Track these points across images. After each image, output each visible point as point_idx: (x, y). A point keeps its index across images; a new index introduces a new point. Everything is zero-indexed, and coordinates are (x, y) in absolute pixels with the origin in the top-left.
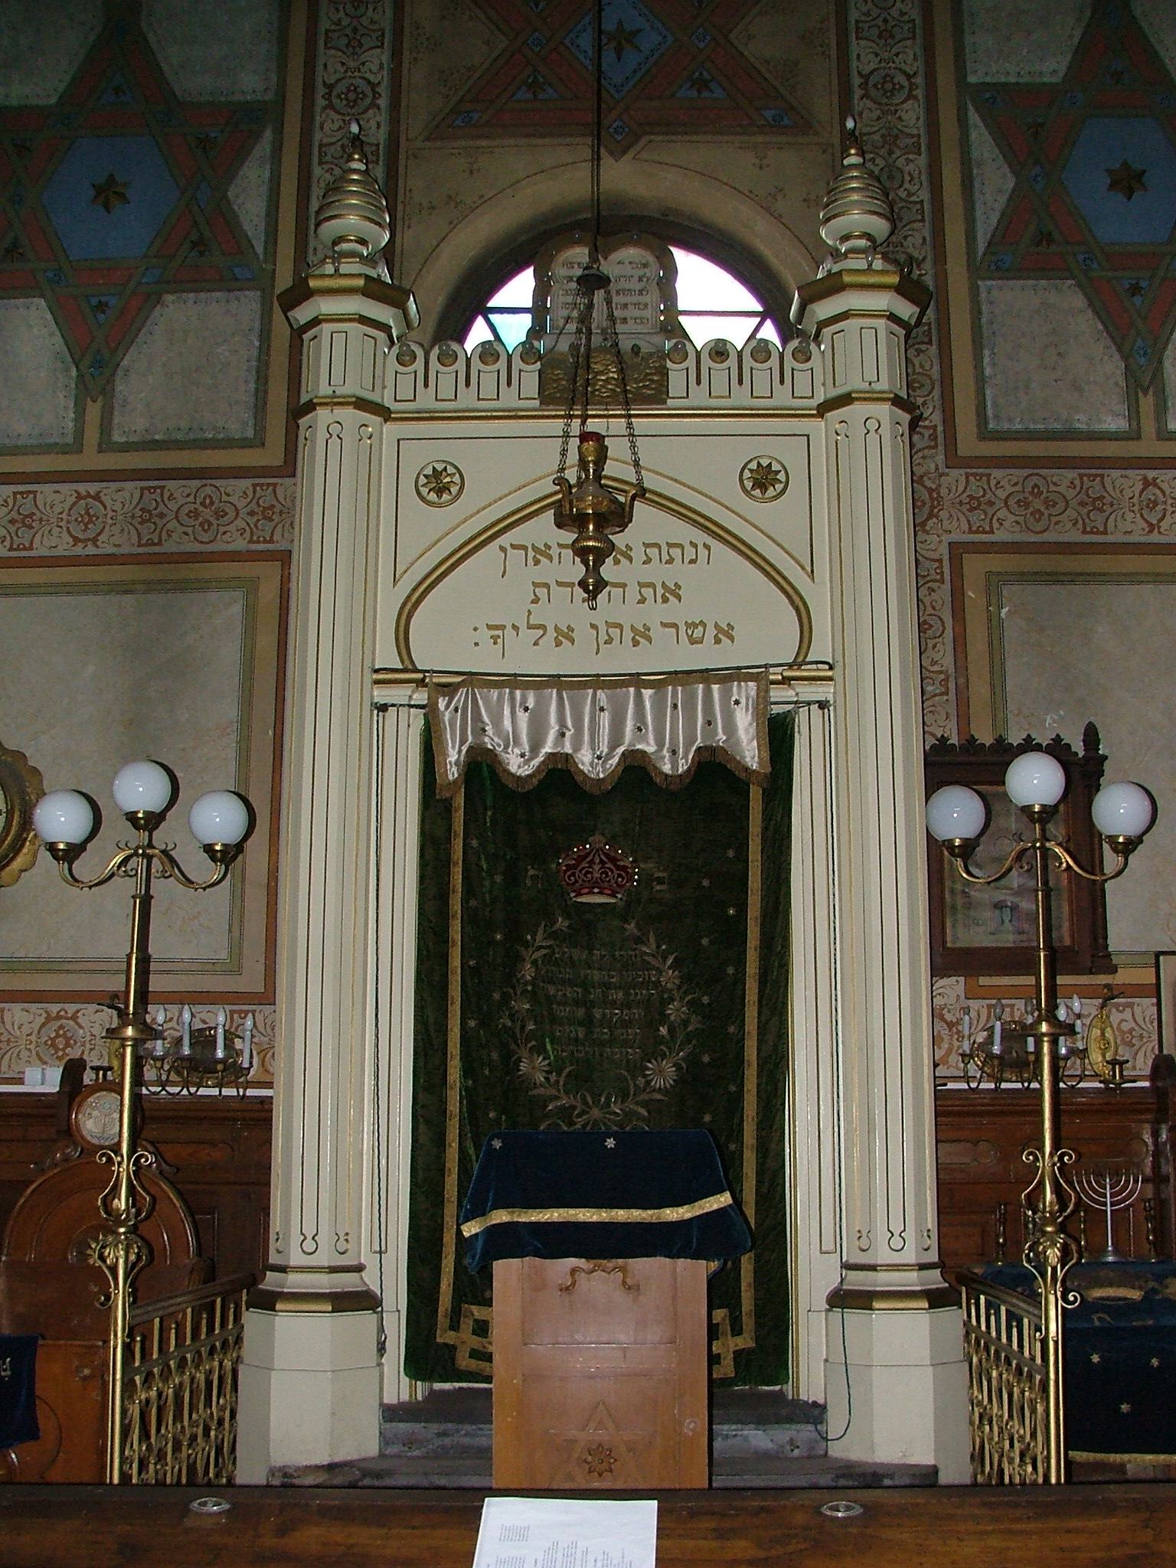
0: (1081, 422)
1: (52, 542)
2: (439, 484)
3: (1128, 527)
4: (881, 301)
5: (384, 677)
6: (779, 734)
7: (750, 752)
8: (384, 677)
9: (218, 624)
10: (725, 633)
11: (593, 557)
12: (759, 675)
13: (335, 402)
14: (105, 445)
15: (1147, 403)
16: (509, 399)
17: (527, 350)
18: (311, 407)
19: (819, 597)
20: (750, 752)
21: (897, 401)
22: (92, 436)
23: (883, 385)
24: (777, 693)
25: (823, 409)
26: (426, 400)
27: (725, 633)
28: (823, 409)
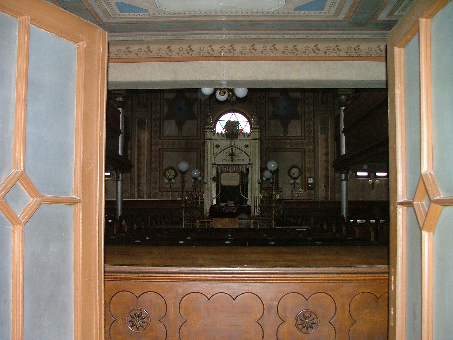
0: (279, 135)
1: (176, 146)
2: (218, 146)
3: (283, 146)
4: (257, 130)
5: (213, 164)
6: (247, 170)
7: (245, 171)
8: (214, 164)
9: (193, 155)
10: (243, 160)
11: (232, 158)
12: (246, 165)
13: (208, 139)
14: (182, 136)
15: (286, 133)
16: (224, 138)
17: (225, 133)
18: (206, 139)
19: (251, 157)
20: (245, 171)
21: (259, 139)
22: (180, 135)
23: (257, 138)
24: (247, 166)
25: (252, 140)
26: (216, 138)
27: (243, 160)
28: (252, 140)
